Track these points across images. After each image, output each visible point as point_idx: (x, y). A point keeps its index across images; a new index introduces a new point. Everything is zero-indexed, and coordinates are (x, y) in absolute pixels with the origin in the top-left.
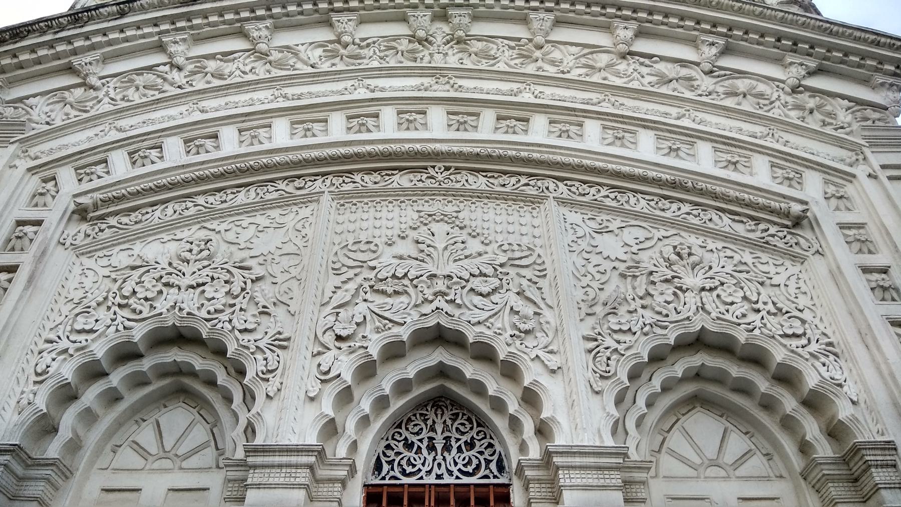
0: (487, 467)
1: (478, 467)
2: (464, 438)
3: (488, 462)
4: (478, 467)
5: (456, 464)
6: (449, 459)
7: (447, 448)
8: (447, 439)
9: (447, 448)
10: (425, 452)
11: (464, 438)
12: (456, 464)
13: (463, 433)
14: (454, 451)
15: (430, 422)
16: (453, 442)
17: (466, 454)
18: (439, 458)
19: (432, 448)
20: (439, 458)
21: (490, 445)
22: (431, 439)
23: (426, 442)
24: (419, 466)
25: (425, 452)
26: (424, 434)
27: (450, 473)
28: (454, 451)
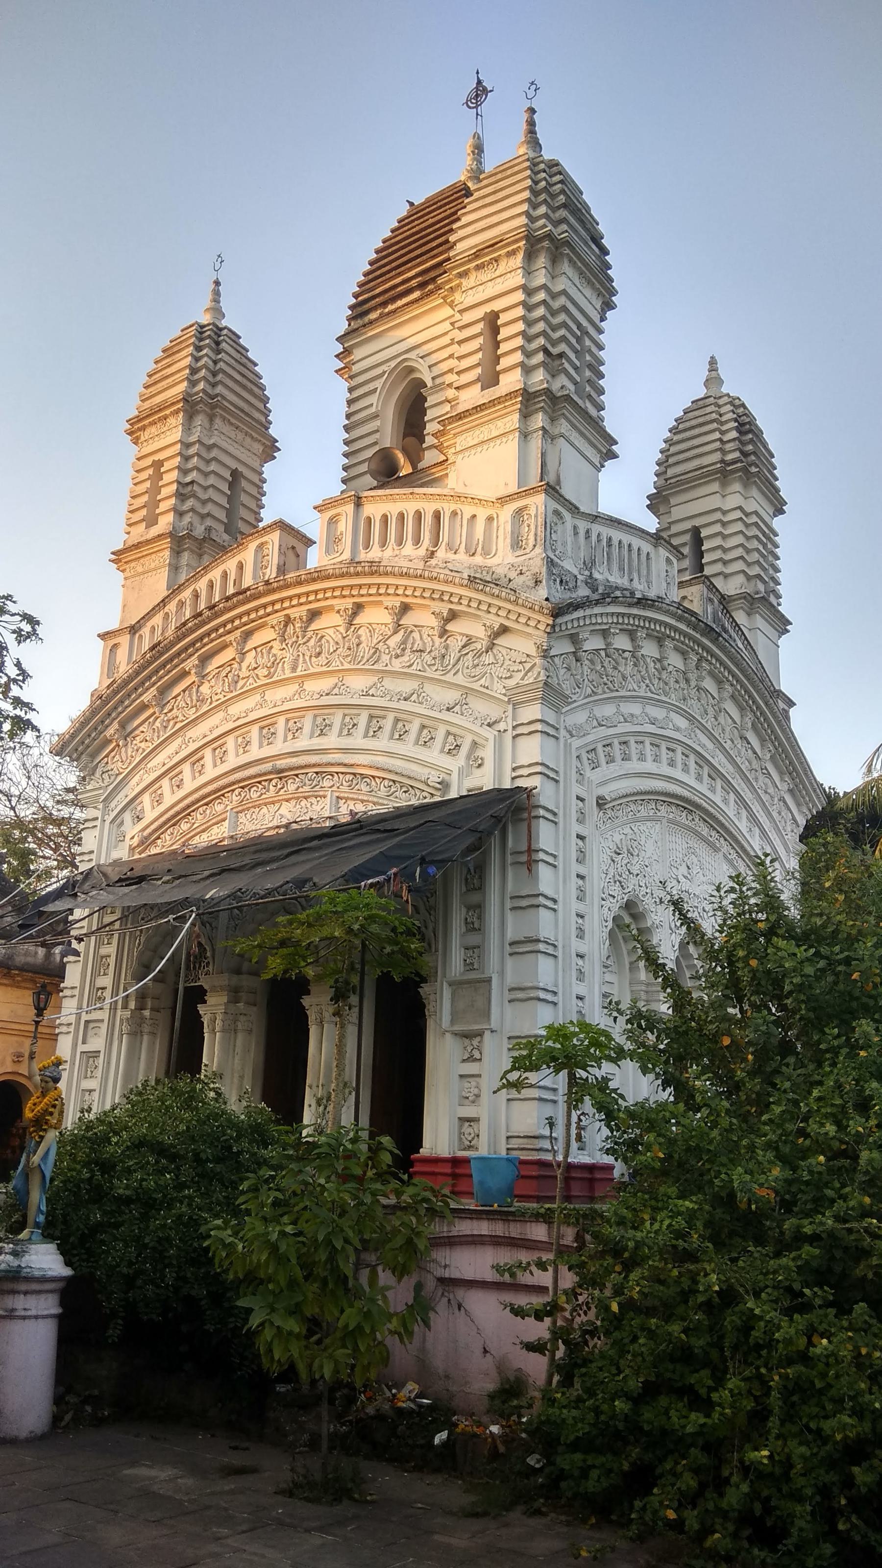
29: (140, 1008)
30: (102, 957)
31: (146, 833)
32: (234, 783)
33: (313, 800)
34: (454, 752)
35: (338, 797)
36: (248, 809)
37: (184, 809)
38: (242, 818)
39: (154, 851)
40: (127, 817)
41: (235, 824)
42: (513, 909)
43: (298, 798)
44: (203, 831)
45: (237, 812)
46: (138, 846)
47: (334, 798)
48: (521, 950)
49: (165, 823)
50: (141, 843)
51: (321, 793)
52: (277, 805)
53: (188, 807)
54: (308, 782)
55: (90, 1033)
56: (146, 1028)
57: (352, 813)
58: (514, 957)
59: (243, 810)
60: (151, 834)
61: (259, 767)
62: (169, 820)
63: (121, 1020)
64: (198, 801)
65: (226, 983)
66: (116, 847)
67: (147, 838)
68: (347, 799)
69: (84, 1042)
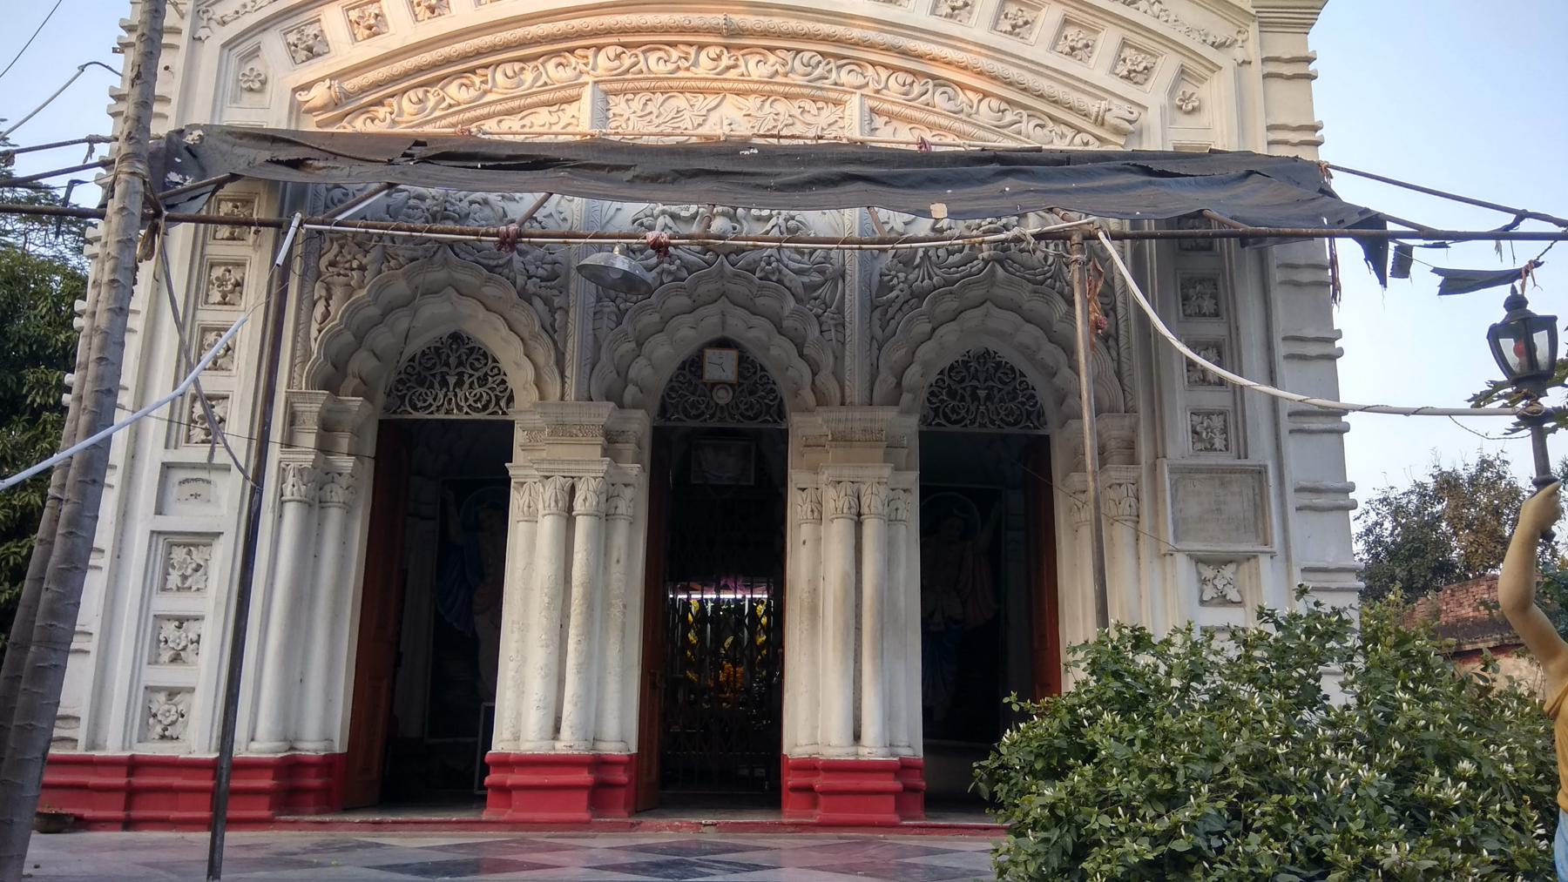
0: (497, 403)
1: (489, 401)
2: (477, 374)
3: (498, 399)
4: (489, 401)
5: (466, 399)
6: (460, 394)
7: (459, 384)
8: (461, 375)
9: (459, 384)
10: (437, 385)
11: (477, 374)
12: (466, 399)
13: (477, 370)
14: (466, 386)
15: (444, 357)
16: (466, 377)
17: (478, 390)
18: (451, 395)
19: (444, 383)
20: (451, 395)
21: (503, 382)
22: (443, 375)
23: (438, 378)
24: (430, 400)
25: (437, 385)
26: (438, 369)
27: (460, 409)
28: (466, 386)
29: (325, 448)
30: (205, 330)
31: (351, 84)
32: (608, 32)
33: (808, 105)
34: (1140, 78)
35: (872, 110)
36: (635, 92)
37: (465, 57)
38: (619, 105)
39: (360, 125)
40: (273, 45)
41: (602, 113)
42: (1290, 357)
43: (768, 95)
44: (509, 113)
45: (607, 93)
46: (324, 108)
47: (867, 109)
48: (1314, 426)
49: (406, 75)
50: (335, 104)
51: (832, 95)
52: (712, 100)
53: (479, 53)
54: (801, 69)
55: (174, 491)
56: (337, 494)
57: (923, 143)
58: (1298, 436)
59: (624, 92)
60: (363, 90)
61: (619, 18)
62: (420, 70)
63: (282, 471)
64: (507, 47)
65: (603, 420)
66: (235, 99)
67: (349, 96)
68: (892, 116)
69: (159, 511)
